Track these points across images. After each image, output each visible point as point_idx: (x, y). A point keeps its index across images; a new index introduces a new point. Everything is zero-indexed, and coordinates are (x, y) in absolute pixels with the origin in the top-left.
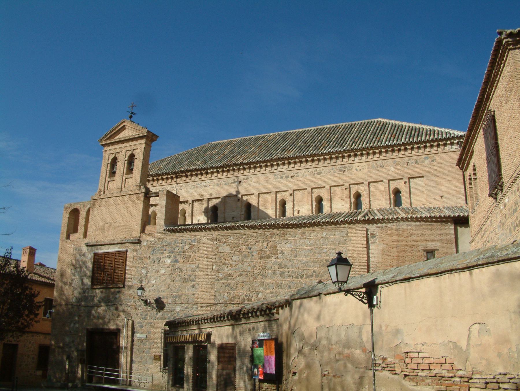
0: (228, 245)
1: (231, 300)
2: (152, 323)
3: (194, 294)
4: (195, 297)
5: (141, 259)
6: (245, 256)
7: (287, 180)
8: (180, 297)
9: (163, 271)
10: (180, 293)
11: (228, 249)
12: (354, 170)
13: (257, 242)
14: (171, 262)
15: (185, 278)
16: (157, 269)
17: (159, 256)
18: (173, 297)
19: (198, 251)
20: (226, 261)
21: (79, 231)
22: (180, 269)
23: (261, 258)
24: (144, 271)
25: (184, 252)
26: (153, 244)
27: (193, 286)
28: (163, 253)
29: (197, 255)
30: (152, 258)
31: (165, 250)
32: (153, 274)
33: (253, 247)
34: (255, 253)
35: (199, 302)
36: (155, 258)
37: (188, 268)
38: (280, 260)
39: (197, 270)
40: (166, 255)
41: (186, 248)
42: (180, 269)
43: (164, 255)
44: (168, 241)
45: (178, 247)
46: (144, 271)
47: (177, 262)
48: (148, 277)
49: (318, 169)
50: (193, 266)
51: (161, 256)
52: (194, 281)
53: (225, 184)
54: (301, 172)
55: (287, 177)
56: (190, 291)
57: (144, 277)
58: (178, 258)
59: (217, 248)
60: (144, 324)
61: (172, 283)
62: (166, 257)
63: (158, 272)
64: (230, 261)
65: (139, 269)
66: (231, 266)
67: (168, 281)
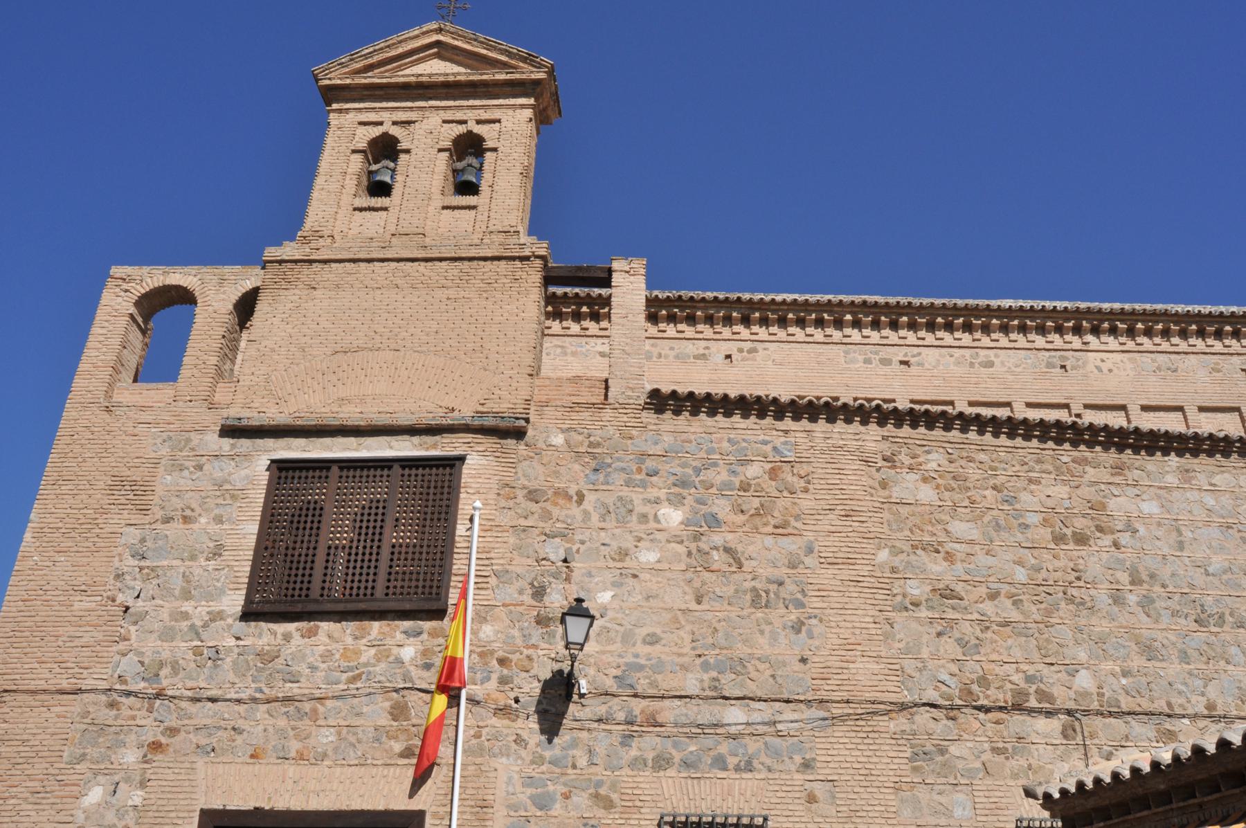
0: (925, 480)
1: (970, 693)
2: (599, 784)
3: (803, 660)
4: (813, 669)
5: (533, 496)
6: (998, 528)
7: (887, 369)
8: (738, 666)
9: (648, 556)
10: (741, 650)
11: (927, 494)
12: (1091, 367)
13: (1030, 481)
14: (686, 523)
15: (754, 589)
16: (615, 545)
17: (625, 492)
18: (706, 667)
19: (806, 491)
20: (927, 538)
21: (185, 372)
22: (727, 550)
23: (1059, 539)
24: (555, 550)
25: (745, 487)
26: (591, 445)
27: (797, 627)
28: (644, 485)
29: (806, 503)
30: (590, 498)
31: (656, 473)
32: (602, 563)
33: (1024, 496)
34: (1033, 519)
35: (836, 696)
36: (610, 500)
37: (765, 553)
38: (1128, 556)
39: (808, 561)
40: (662, 494)
41: (753, 471)
42: (727, 550)
43: (653, 493)
44: (668, 439)
45: (715, 465)
46: (555, 550)
47: (714, 521)
48: (576, 576)
49: (982, 353)
50: (791, 545)
51: (637, 497)
52: (800, 605)
53: (677, 357)
54: (930, 355)
55: (885, 362)
56: (786, 648)
57: (556, 576)
58: (722, 508)
59: (884, 485)
60: (561, 789)
61: (693, 606)
62: (657, 501)
63: (623, 554)
64: (942, 537)
65: (534, 539)
66: (949, 557)
67: (678, 597)
